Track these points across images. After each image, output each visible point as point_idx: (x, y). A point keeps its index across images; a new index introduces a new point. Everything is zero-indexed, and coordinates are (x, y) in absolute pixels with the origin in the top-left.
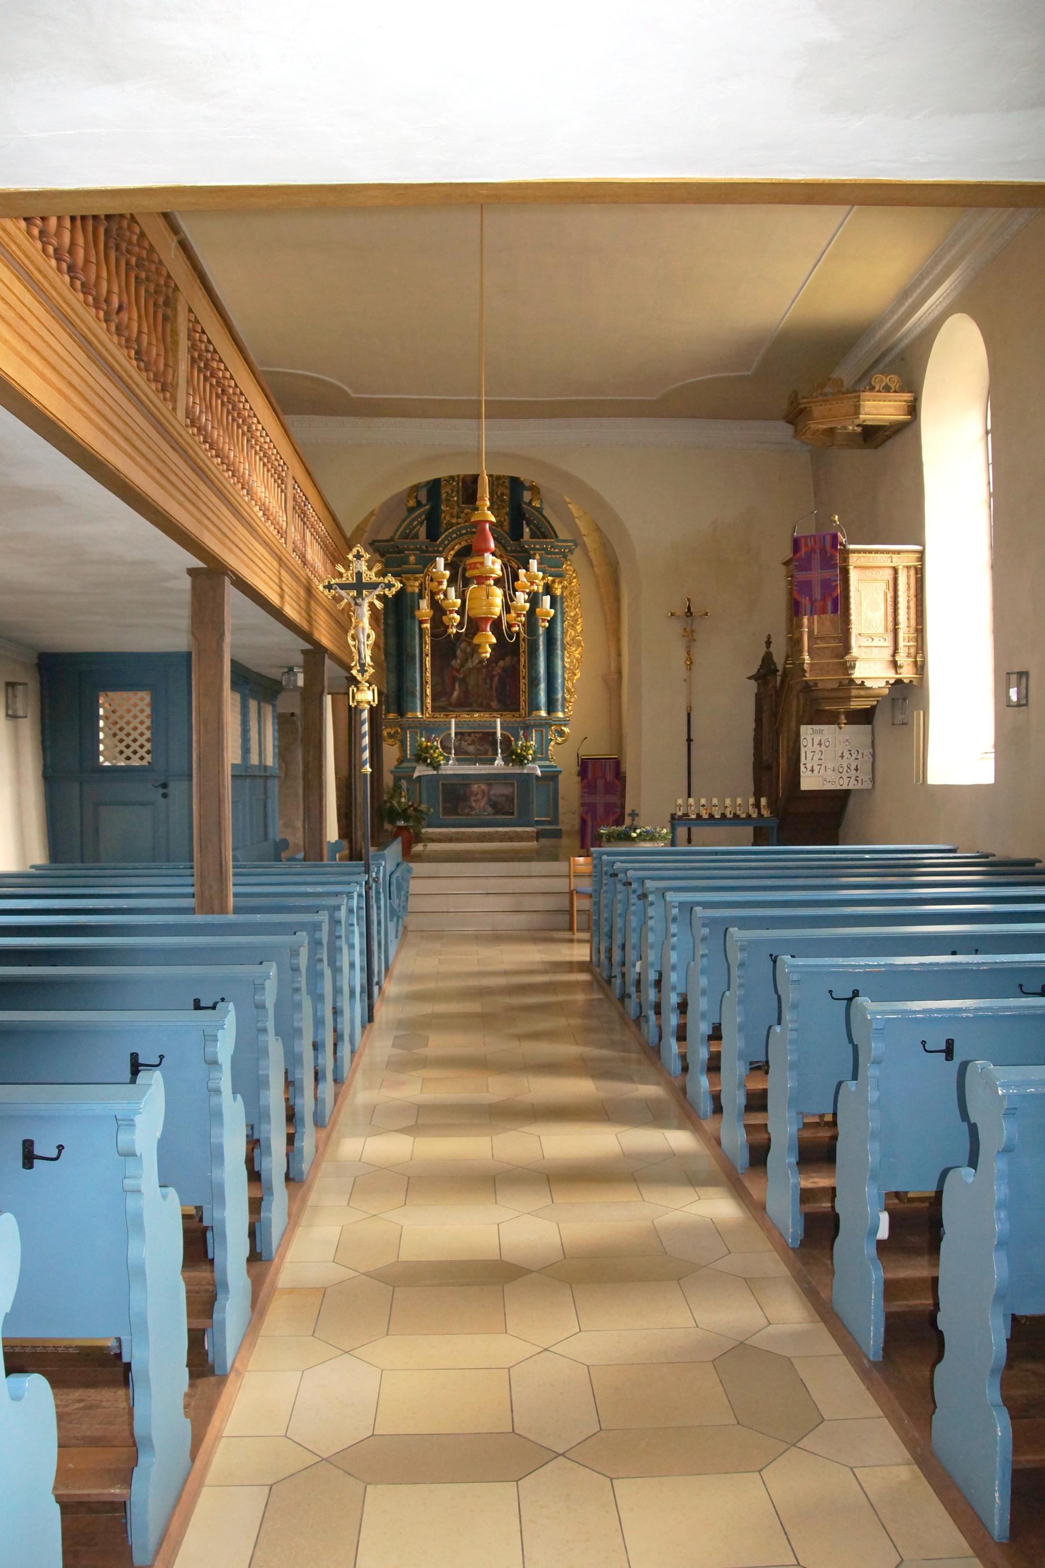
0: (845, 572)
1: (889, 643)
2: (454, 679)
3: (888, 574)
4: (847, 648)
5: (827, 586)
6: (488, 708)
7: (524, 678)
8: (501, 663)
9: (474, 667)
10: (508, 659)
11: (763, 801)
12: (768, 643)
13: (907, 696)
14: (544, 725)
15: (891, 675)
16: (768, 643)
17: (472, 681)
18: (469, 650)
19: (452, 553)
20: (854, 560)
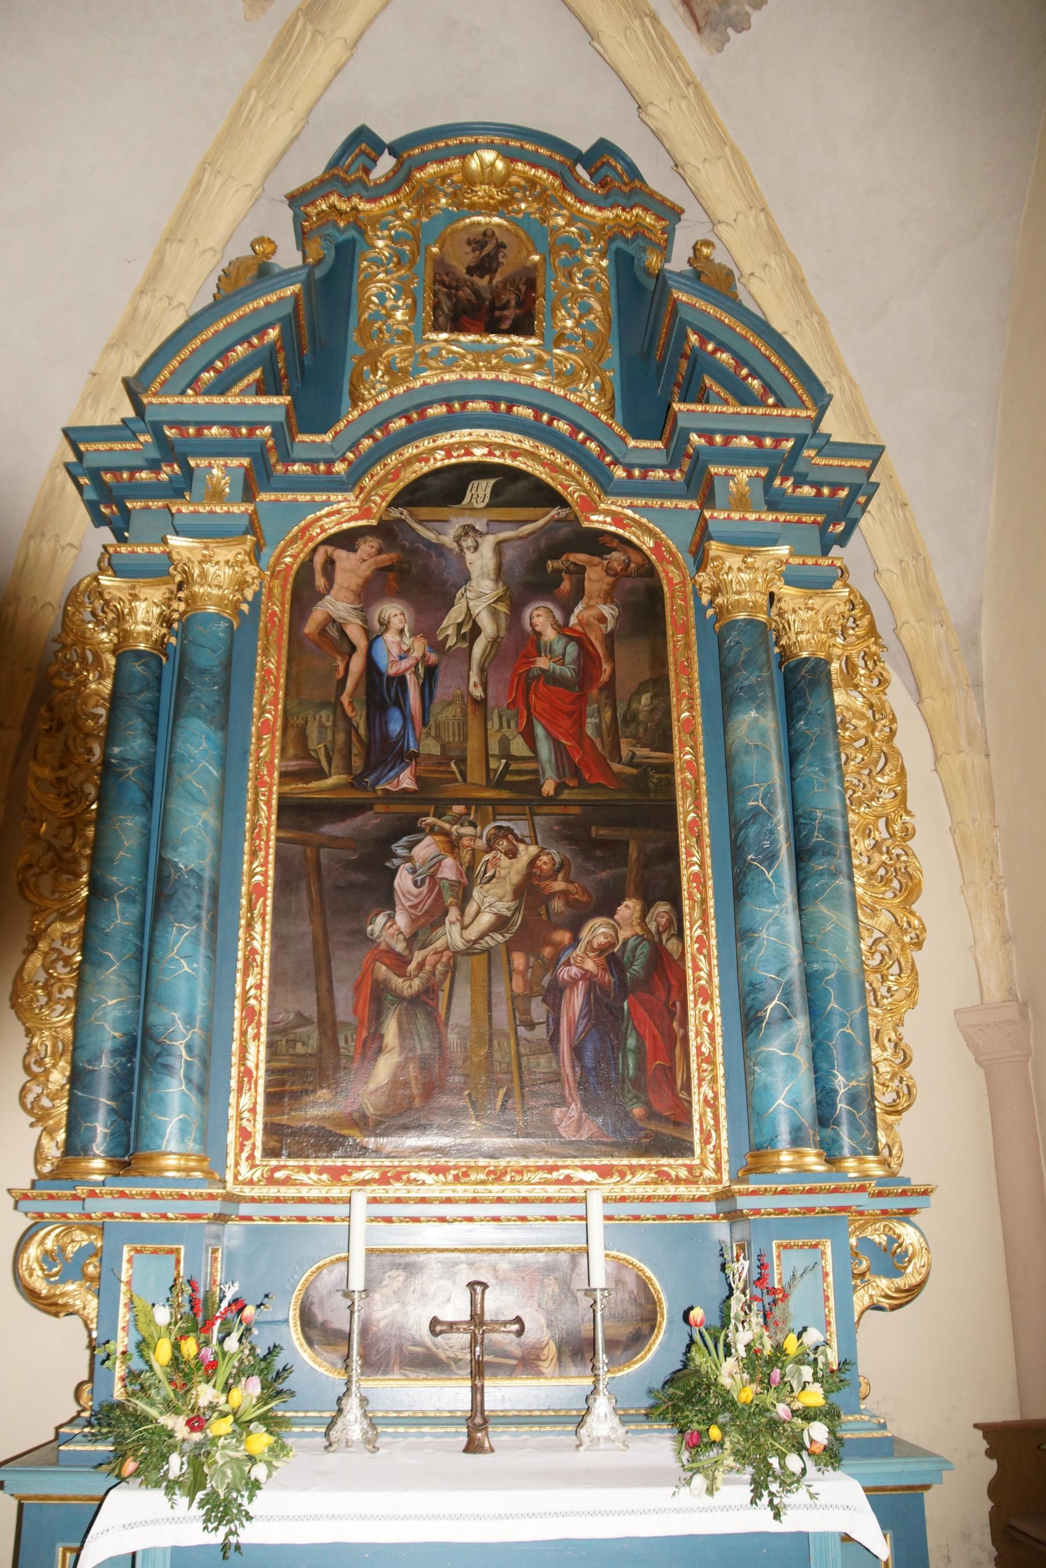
2: (378, 999)
7: (704, 995)
8: (597, 931)
9: (470, 950)
10: (629, 909)
18: (449, 870)
19: (393, 489)
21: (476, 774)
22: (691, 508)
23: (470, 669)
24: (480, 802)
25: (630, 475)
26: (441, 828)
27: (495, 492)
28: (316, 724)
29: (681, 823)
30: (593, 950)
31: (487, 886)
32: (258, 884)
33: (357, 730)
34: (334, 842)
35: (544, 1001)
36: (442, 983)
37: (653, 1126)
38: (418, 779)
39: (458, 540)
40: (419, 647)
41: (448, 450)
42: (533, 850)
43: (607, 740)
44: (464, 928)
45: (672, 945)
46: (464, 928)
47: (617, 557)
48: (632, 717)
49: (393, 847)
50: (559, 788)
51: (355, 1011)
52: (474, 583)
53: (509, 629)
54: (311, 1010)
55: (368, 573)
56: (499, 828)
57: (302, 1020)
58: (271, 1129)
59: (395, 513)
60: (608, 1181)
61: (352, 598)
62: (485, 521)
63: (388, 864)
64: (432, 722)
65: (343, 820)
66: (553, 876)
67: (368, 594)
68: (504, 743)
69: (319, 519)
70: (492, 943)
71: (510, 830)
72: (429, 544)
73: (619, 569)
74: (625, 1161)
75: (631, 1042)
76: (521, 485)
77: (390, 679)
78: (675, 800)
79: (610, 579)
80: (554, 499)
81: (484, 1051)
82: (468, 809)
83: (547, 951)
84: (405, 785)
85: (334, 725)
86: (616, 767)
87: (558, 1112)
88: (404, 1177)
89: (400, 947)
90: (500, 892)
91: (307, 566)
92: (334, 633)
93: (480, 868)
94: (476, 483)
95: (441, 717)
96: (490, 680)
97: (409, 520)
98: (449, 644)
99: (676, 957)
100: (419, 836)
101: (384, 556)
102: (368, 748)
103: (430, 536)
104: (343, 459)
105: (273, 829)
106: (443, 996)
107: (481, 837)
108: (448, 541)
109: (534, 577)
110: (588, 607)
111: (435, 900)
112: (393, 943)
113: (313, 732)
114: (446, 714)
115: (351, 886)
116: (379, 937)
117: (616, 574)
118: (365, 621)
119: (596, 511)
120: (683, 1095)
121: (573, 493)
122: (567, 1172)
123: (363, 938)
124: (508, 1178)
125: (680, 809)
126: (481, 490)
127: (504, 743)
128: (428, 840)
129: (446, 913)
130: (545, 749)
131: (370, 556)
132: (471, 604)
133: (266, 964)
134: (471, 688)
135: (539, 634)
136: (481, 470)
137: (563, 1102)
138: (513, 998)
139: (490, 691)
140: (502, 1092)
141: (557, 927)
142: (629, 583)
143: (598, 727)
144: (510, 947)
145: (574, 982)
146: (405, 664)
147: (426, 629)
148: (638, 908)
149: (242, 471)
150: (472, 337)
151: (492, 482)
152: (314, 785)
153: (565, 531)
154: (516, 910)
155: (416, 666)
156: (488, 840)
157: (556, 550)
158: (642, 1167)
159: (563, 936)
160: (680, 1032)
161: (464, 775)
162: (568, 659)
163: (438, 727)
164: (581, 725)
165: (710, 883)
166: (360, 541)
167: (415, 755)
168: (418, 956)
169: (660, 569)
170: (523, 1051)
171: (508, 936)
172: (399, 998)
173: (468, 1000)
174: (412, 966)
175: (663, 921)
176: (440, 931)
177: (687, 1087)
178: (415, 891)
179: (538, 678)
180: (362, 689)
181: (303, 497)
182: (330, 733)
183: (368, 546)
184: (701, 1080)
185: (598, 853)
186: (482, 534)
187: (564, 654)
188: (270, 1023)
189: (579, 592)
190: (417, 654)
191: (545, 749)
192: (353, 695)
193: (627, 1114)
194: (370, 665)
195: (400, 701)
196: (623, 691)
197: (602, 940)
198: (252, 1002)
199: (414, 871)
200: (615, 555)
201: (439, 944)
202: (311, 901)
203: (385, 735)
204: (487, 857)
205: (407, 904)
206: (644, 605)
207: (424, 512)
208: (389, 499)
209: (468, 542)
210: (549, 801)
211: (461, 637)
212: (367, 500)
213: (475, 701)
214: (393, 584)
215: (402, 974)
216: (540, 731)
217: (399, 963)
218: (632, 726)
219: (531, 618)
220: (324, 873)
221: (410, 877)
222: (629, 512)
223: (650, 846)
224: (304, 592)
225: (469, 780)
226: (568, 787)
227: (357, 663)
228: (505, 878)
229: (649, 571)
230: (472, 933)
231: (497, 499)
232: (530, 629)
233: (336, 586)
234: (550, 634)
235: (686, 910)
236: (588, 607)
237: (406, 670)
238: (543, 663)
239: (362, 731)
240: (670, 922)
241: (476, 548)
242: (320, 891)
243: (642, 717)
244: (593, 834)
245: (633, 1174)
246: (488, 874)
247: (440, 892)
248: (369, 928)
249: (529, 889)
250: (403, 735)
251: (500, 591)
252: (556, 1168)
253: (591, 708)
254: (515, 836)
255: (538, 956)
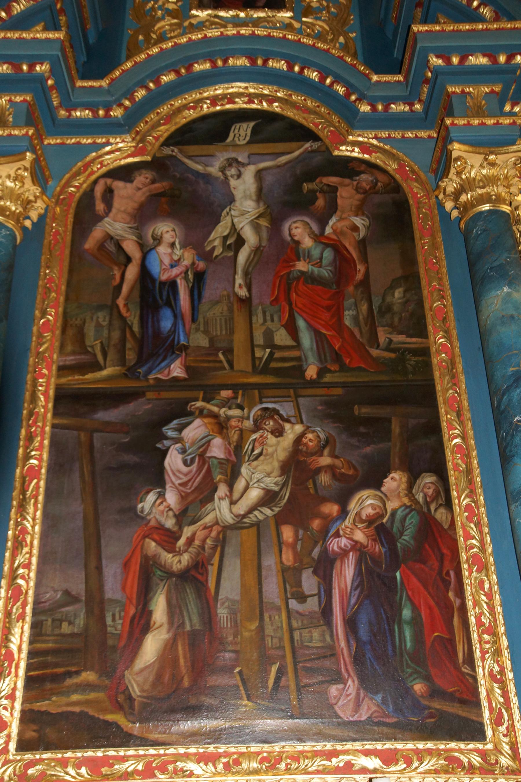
2: (147, 576)
8: (365, 502)
9: (240, 524)
10: (395, 481)
17: (230, 584)
18: (217, 449)
19: (165, 131)
21: (242, 362)
22: (430, 137)
23: (235, 273)
24: (246, 387)
25: (374, 108)
26: (210, 411)
27: (254, 131)
28: (93, 324)
29: (440, 400)
30: (362, 521)
31: (255, 463)
32: (32, 467)
33: (131, 328)
34: (107, 427)
35: (315, 572)
36: (212, 556)
37: (436, 705)
38: (188, 368)
39: (223, 170)
40: (188, 257)
41: (214, 100)
42: (299, 428)
43: (365, 329)
44: (233, 503)
45: (441, 515)
46: (233, 503)
47: (365, 179)
48: (386, 309)
49: (164, 429)
50: (321, 372)
51: (123, 589)
52: (237, 203)
53: (270, 240)
54: (79, 588)
55: (143, 199)
56: (266, 409)
57: (70, 598)
58: (27, 717)
59: (167, 151)
60: (393, 769)
61: (128, 219)
62: (246, 154)
63: (159, 445)
64: (201, 319)
65: (116, 406)
66: (319, 453)
67: (142, 216)
68: (269, 335)
69: (101, 156)
70: (261, 517)
71: (276, 412)
72: (197, 174)
73: (368, 187)
74: (410, 745)
75: (407, 613)
76: (277, 125)
77: (163, 284)
78: (433, 380)
79: (359, 196)
81: (254, 626)
82: (236, 393)
83: (316, 524)
84: (175, 374)
85: (110, 324)
86: (375, 352)
87: (334, 690)
88: (171, 767)
89: (170, 523)
90: (268, 468)
91: (88, 196)
92: (111, 247)
93: (247, 447)
94: (238, 125)
95: (210, 314)
96: (254, 282)
97: (180, 156)
98: (216, 253)
99: (446, 527)
100: (189, 419)
101: (157, 185)
102: (141, 343)
103: (199, 168)
104: (120, 105)
105: (49, 415)
106: (213, 571)
107: (248, 418)
108: (214, 170)
109: (291, 196)
110: (341, 219)
111: (204, 478)
112: (162, 520)
113: (90, 331)
114: (213, 312)
115: (123, 467)
116: (149, 514)
117: (365, 192)
118: (140, 237)
119: (344, 142)
120: (466, 670)
121: (324, 133)
122: (347, 758)
123: (131, 515)
124: (282, 766)
125: (438, 387)
126: (243, 131)
127: (269, 335)
128: (198, 422)
129: (215, 490)
130: (306, 339)
131: (145, 185)
132: (236, 220)
133: (36, 543)
134: (237, 289)
135: (298, 243)
136: (243, 116)
137: (338, 678)
138: (284, 570)
139: (254, 290)
140: (274, 669)
141: (324, 500)
142: (377, 199)
143: (356, 319)
144: (280, 520)
145: (344, 553)
146: (175, 271)
147: (195, 241)
148: (404, 480)
149: (25, 105)
150: (231, 13)
151: (252, 124)
152: (89, 376)
153: (318, 159)
154: (284, 485)
155: (186, 272)
156: (255, 421)
157: (310, 176)
158: (429, 752)
159: (333, 509)
160: (457, 602)
161: (231, 364)
162: (324, 262)
163: (206, 323)
164: (340, 318)
165: (474, 454)
166: (136, 174)
167: (185, 348)
168: (188, 531)
169: (404, 185)
170: (295, 624)
171: (277, 509)
172: (169, 574)
173: (237, 573)
174: (182, 542)
175: (430, 492)
176: (209, 506)
177: (470, 660)
178: (185, 469)
179: (298, 279)
180: (137, 293)
181: (87, 141)
182: (105, 333)
183: (142, 178)
184: (484, 653)
185: (362, 429)
186: (244, 165)
187: (321, 258)
188: (36, 602)
189: (332, 207)
190: (187, 262)
191: (306, 339)
192: (128, 298)
193: (408, 690)
194: (144, 273)
195: (172, 300)
196: (377, 286)
197: (370, 511)
198: (20, 581)
199: (183, 451)
200: (363, 176)
201: (208, 519)
202: (83, 481)
203: (157, 333)
204: (254, 436)
205: (177, 482)
206: (393, 216)
207: (193, 149)
208: (162, 140)
209: (233, 171)
210: (313, 384)
211: (227, 248)
212: (142, 140)
213: (241, 300)
214: (165, 206)
215: (171, 549)
216: (301, 323)
217: (168, 539)
218: (388, 316)
219: (290, 230)
220: (97, 455)
221: (180, 456)
222: (374, 142)
223: (412, 422)
224: (86, 213)
225: (236, 367)
226: (330, 371)
227: (132, 272)
228: (272, 455)
229: (395, 188)
230: (241, 508)
231: (256, 137)
232: (289, 239)
233: (114, 210)
234: (307, 242)
235: (452, 480)
236: (341, 219)
237: (177, 276)
238: (301, 266)
239: (136, 328)
240: (436, 495)
241: (239, 176)
242: (93, 473)
243: (396, 308)
244: (356, 413)
245: (421, 761)
246: (256, 452)
247: (209, 471)
248: (140, 506)
249: (296, 466)
250: (174, 330)
251: (262, 209)
252: (335, 754)
253: (348, 302)
254: (281, 416)
255: (306, 529)
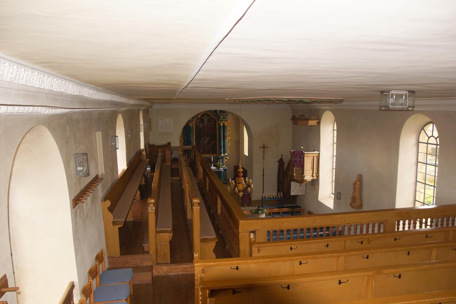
0: (304, 158)
1: (311, 172)
3: (312, 158)
4: (303, 173)
5: (300, 161)
6: (210, 153)
11: (281, 193)
12: (282, 156)
13: (315, 183)
14: (223, 158)
15: (312, 178)
16: (282, 156)
20: (305, 155)
67: (199, 122)
80: (210, 116)
109: (209, 121)
126: (206, 115)
